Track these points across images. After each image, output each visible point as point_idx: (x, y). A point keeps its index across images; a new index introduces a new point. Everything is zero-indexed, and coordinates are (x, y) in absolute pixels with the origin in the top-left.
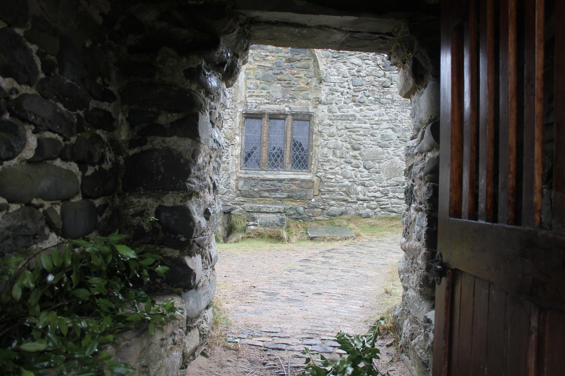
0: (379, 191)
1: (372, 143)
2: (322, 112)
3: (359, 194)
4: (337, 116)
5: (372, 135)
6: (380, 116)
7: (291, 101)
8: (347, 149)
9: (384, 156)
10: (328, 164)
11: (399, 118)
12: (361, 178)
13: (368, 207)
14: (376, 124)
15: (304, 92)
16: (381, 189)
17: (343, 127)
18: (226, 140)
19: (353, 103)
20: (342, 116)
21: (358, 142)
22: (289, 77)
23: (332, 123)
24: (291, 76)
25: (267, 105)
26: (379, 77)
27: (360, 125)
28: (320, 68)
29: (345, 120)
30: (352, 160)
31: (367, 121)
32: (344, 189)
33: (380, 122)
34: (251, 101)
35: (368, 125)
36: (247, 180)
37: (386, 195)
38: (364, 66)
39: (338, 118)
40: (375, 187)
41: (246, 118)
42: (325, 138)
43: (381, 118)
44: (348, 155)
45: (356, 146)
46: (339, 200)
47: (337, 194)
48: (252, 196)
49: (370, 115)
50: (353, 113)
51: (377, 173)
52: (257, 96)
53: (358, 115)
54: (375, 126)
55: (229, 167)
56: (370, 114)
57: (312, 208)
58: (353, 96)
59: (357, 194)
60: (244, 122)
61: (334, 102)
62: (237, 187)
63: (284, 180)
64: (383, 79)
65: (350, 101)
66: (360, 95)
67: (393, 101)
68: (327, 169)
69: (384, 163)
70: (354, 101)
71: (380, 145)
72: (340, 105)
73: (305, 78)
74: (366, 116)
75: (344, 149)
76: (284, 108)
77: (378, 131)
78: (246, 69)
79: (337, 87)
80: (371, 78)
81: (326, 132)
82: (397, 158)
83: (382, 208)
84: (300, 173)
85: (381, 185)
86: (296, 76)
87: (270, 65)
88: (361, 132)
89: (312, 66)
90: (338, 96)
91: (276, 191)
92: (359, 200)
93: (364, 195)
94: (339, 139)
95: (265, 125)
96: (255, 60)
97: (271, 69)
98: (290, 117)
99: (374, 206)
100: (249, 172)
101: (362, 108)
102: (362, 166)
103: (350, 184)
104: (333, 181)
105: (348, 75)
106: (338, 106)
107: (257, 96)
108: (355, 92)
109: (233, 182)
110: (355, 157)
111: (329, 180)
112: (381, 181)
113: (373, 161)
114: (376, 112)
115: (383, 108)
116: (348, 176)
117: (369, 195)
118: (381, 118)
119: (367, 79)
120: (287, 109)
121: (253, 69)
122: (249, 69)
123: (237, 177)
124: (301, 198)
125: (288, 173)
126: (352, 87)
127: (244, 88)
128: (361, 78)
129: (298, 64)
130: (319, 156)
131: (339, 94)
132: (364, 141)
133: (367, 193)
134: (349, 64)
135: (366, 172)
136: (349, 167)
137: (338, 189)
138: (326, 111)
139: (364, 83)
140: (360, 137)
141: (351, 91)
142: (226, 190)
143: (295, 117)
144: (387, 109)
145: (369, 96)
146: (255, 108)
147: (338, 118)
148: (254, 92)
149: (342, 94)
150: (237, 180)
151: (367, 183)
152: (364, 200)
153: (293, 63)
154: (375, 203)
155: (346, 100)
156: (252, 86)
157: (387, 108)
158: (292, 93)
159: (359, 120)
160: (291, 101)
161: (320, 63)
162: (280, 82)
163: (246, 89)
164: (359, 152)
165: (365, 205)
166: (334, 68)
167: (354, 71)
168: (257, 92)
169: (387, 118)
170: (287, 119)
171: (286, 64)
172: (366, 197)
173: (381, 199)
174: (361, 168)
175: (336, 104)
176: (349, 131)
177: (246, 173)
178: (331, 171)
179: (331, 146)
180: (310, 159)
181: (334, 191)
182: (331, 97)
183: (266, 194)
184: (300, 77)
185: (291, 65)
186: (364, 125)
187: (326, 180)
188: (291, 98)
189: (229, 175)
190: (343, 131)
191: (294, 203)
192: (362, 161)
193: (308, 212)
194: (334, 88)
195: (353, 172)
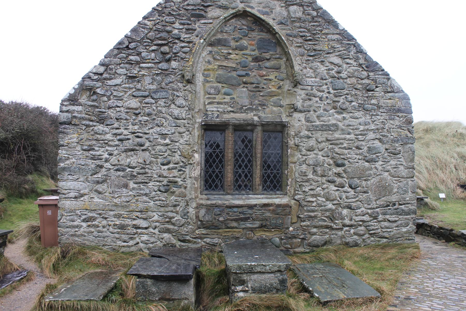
0: (368, 213)
1: (358, 157)
2: (297, 122)
3: (345, 219)
4: (317, 126)
5: (358, 148)
6: (366, 125)
7: (260, 108)
8: (329, 165)
9: (371, 172)
10: (307, 184)
11: (386, 127)
12: (346, 200)
13: (355, 234)
14: (361, 135)
15: (275, 98)
16: (369, 211)
17: (324, 139)
18: (182, 158)
19: (334, 111)
20: (322, 126)
21: (342, 157)
22: (257, 79)
23: (310, 135)
24: (259, 79)
25: (232, 114)
26: (362, 79)
27: (343, 136)
28: (295, 68)
29: (325, 131)
30: (336, 179)
31: (351, 131)
32: (328, 214)
33: (365, 132)
34: (212, 109)
35: (352, 136)
36: (210, 208)
37: (375, 218)
38: (345, 66)
39: (317, 129)
40: (363, 209)
41: (205, 130)
42: (303, 153)
43: (366, 127)
44: (330, 173)
45: (340, 162)
46: (322, 227)
47: (319, 221)
48: (217, 228)
49: (354, 123)
50: (334, 122)
51: (365, 192)
52: (218, 103)
53: (340, 124)
54: (360, 137)
55: (187, 193)
56: (354, 122)
57: (290, 238)
58: (334, 102)
59: (343, 219)
60: (203, 136)
61: (312, 109)
62: (197, 217)
63: (255, 205)
64: (366, 81)
65: (331, 108)
66: (342, 101)
67: (379, 107)
68: (307, 190)
69: (372, 181)
70: (335, 108)
71: (367, 159)
72: (319, 112)
73: (277, 80)
74: (350, 126)
75: (326, 165)
76: (253, 117)
77: (363, 143)
78: (205, 70)
79: (315, 91)
80: (354, 80)
81: (304, 146)
82: (386, 174)
83: (371, 234)
84: (274, 196)
85: (370, 207)
86: (265, 78)
87: (234, 65)
88: (345, 145)
89: (283, 66)
90: (317, 102)
91: (246, 219)
92: (344, 225)
93: (351, 220)
94: (320, 153)
95: (230, 138)
96: (215, 59)
97: (235, 70)
98: (259, 128)
99: (362, 232)
100: (212, 197)
102: (347, 185)
103: (334, 207)
104: (314, 204)
105: (327, 77)
106: (317, 113)
107: (218, 103)
108: (336, 96)
109: (192, 211)
110: (339, 175)
111: (310, 204)
112: (369, 203)
113: (359, 178)
114: (360, 120)
115: (368, 115)
116: (332, 198)
117: (357, 220)
118: (366, 127)
119: (349, 81)
120: (256, 118)
121: (213, 70)
122: (208, 70)
123: (197, 204)
124: (277, 227)
125: (259, 196)
126: (332, 91)
127: (202, 93)
128: (341, 80)
129: (268, 64)
130: (297, 175)
131: (317, 99)
132: (348, 156)
133: (354, 217)
135: (352, 192)
136: (333, 187)
137: (320, 214)
138: (303, 120)
139: (346, 86)
140: (344, 150)
141: (331, 95)
142: (183, 221)
143: (265, 128)
144: (373, 117)
145: (352, 102)
146: (217, 117)
147: (317, 129)
148: (215, 98)
149: (321, 99)
150: (197, 208)
151: (353, 204)
152: (351, 226)
153: (260, 63)
154: (363, 228)
155: (325, 107)
156: (212, 91)
157: (372, 115)
158: (261, 98)
159: (342, 130)
160: (260, 108)
161: (294, 63)
162: (246, 85)
163: (205, 95)
164: (343, 168)
165: (352, 231)
166: (311, 68)
167: (333, 72)
168: (219, 98)
169: (373, 127)
170: (256, 130)
171: (252, 64)
172: (353, 222)
173: (370, 223)
174: (347, 188)
175: (315, 111)
176: (331, 144)
177: (208, 199)
178: (312, 192)
179: (311, 162)
180: (284, 179)
181: (315, 217)
182: (308, 103)
183: (234, 224)
184: (270, 80)
185: (259, 65)
186: (348, 136)
187: (306, 204)
188: (260, 104)
189: (187, 202)
190: (324, 143)
191: (267, 234)
192: (347, 179)
193: (285, 244)
194: (311, 92)
195: (337, 193)
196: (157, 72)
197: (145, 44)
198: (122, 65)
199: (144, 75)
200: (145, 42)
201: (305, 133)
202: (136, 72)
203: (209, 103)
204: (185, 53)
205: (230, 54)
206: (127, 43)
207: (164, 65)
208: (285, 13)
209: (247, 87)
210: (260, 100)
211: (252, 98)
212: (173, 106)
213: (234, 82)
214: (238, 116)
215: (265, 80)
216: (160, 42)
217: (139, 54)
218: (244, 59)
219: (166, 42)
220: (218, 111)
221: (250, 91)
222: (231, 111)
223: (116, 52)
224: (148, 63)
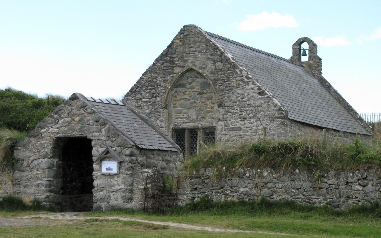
4: (230, 129)
7: (202, 120)
15: (210, 114)
19: (239, 119)
23: (227, 133)
25: (187, 123)
31: (249, 130)
34: (177, 121)
35: (249, 133)
38: (246, 94)
39: (229, 130)
49: (250, 126)
50: (239, 125)
52: (181, 118)
53: (242, 127)
66: (244, 114)
72: (231, 121)
76: (198, 124)
90: (230, 115)
97: (189, 100)
101: (245, 122)
107: (181, 118)
108: (241, 111)
114: (254, 124)
120: (200, 125)
126: (239, 109)
134: (236, 94)
139: (246, 105)
141: (238, 111)
146: (180, 126)
148: (179, 116)
153: (202, 95)
159: (244, 130)
160: (202, 120)
162: (195, 108)
167: (239, 98)
171: (198, 96)
184: (207, 104)
186: (247, 133)
196: (150, 103)
197: (144, 89)
198: (133, 100)
199: (144, 105)
200: (144, 88)
202: (140, 104)
203: (176, 118)
204: (163, 93)
205: (186, 91)
206: (135, 89)
207: (153, 100)
209: (195, 109)
210: (202, 115)
211: (197, 114)
212: (158, 121)
213: (188, 107)
214: (187, 124)
215: (205, 104)
216: (151, 88)
217: (141, 94)
218: (193, 94)
219: (154, 87)
220: (180, 122)
221: (197, 111)
222: (187, 122)
223: (130, 93)
224: (146, 99)
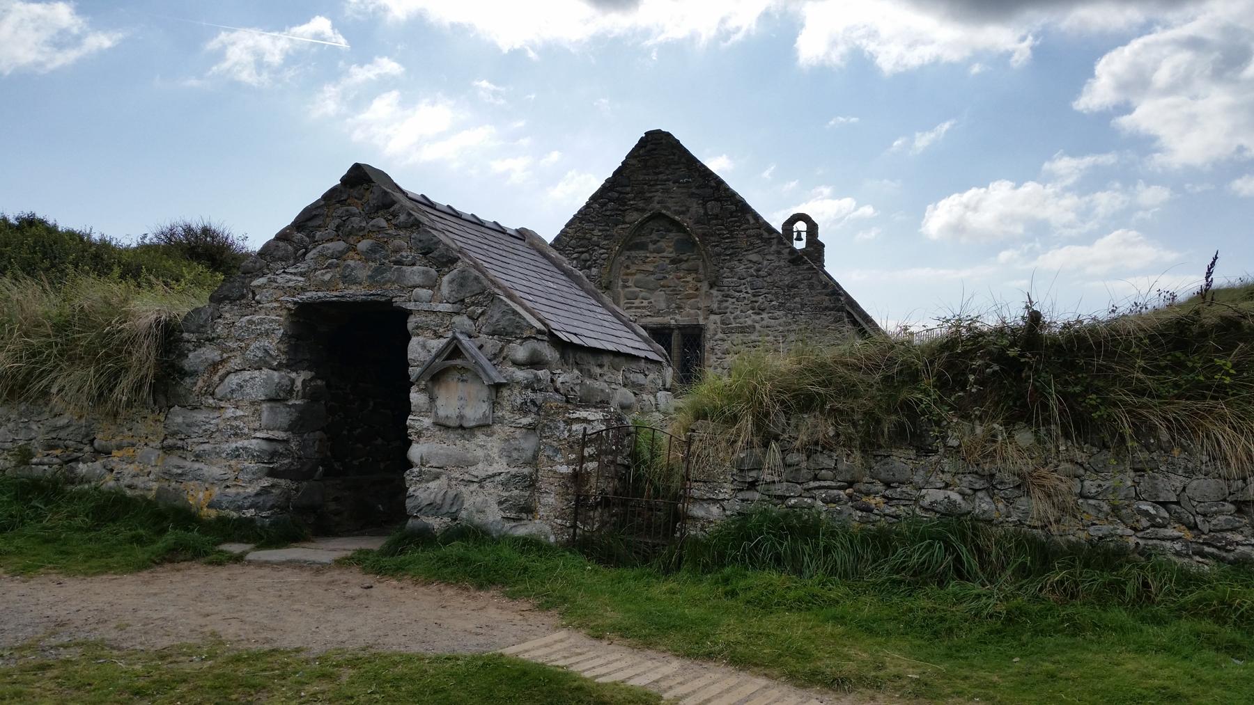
76: (670, 320)
79: (732, 292)
97: (653, 273)
114: (781, 321)
120: (673, 322)
129: (684, 266)
168: (637, 303)
201: (720, 335)
208: (702, 211)
211: (668, 301)
213: (651, 286)
214: (649, 319)
